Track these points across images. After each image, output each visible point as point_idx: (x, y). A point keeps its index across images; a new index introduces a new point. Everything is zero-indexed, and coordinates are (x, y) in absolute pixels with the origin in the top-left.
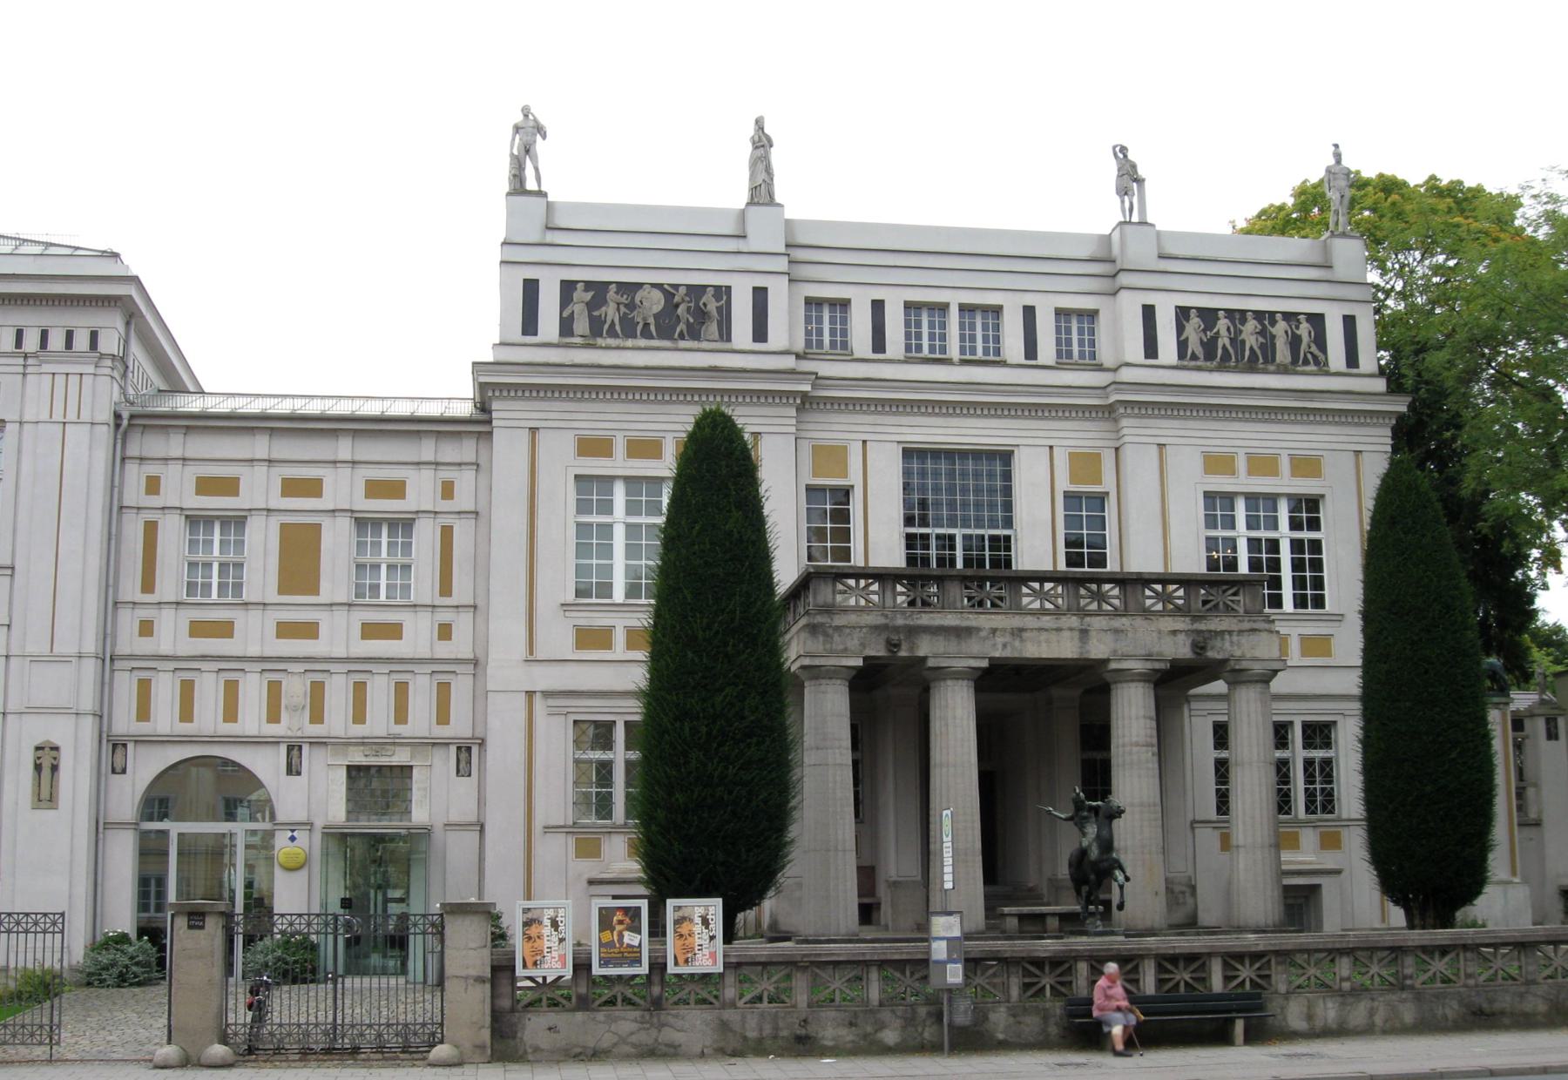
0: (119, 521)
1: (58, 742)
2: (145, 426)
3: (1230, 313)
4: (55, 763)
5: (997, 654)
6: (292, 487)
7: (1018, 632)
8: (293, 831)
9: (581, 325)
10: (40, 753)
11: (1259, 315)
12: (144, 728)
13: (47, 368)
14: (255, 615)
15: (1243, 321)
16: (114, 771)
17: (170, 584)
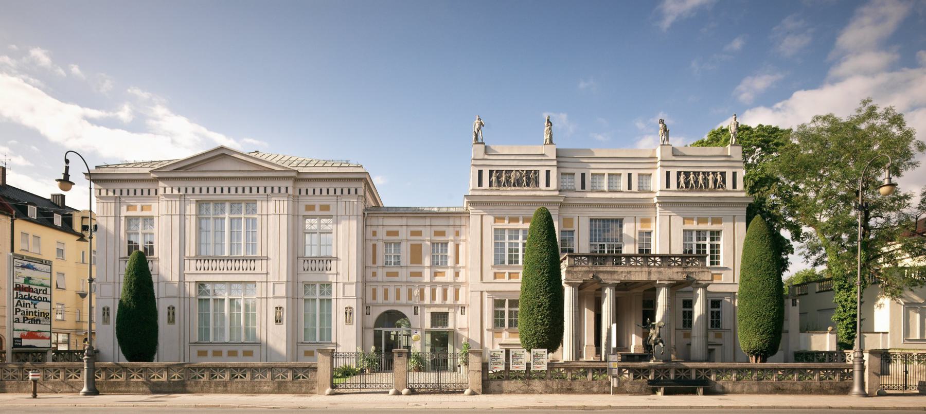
0: (366, 242)
1: (351, 306)
2: (371, 216)
3: (694, 173)
5: (623, 279)
6: (413, 233)
7: (629, 272)
11: (704, 173)
12: (375, 302)
13: (343, 200)
14: (404, 270)
15: (699, 175)
16: (367, 314)
17: (380, 261)
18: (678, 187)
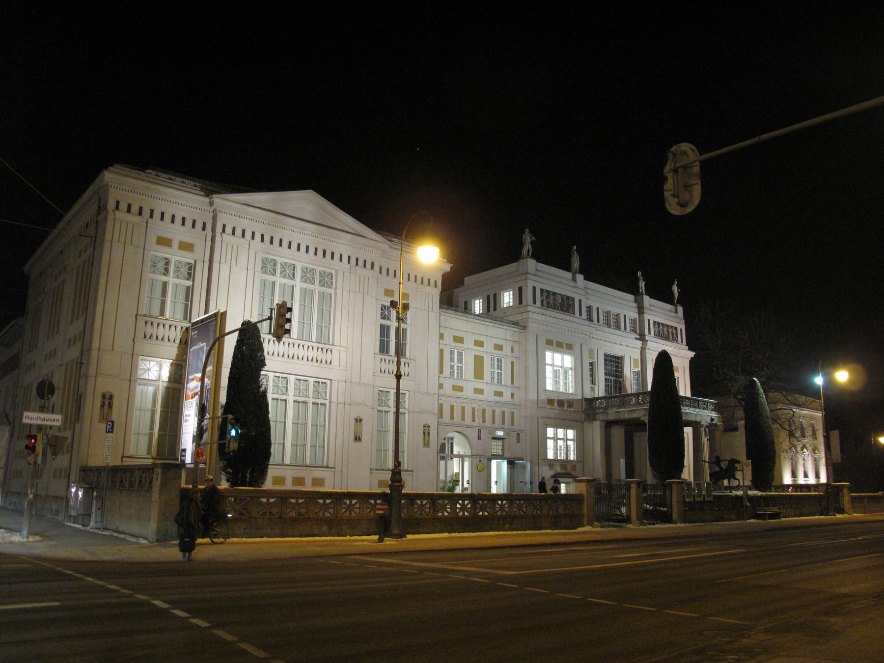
10: (425, 428)
18: (655, 335)
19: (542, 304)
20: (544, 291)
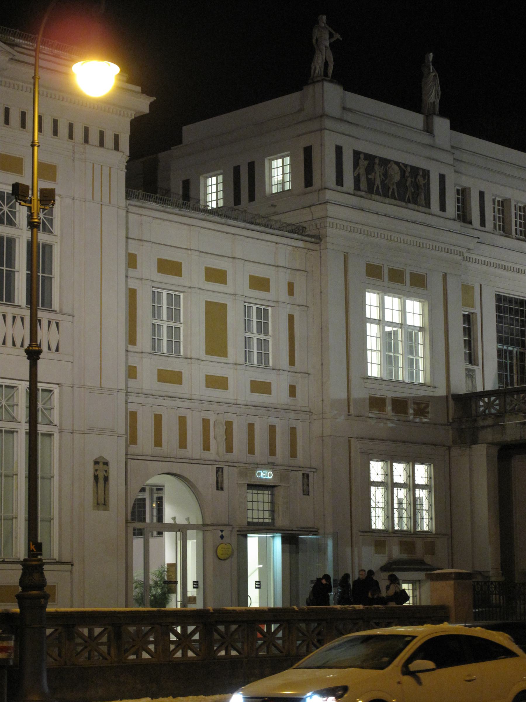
1: (107, 458)
4: (106, 475)
8: (222, 531)
9: (363, 185)
10: (97, 467)
19: (357, 187)
20: (362, 156)
